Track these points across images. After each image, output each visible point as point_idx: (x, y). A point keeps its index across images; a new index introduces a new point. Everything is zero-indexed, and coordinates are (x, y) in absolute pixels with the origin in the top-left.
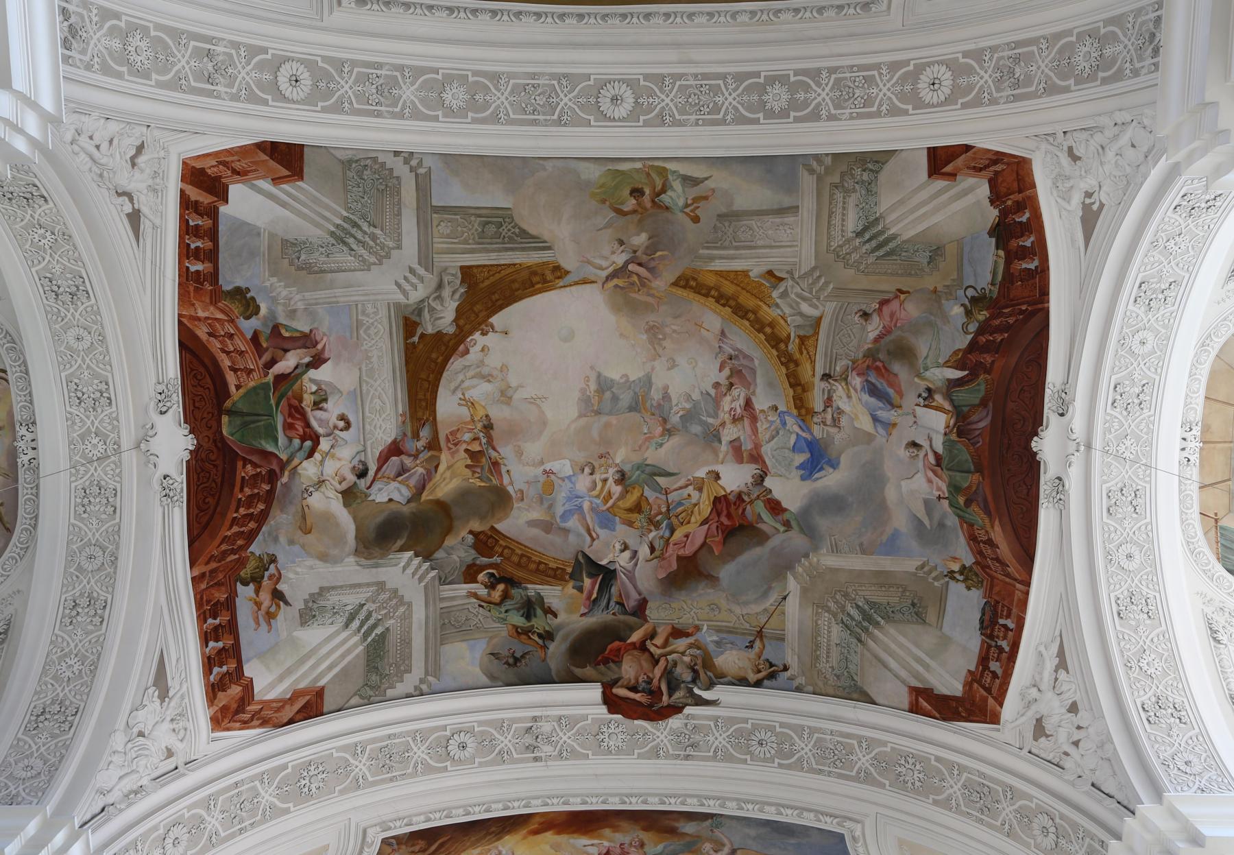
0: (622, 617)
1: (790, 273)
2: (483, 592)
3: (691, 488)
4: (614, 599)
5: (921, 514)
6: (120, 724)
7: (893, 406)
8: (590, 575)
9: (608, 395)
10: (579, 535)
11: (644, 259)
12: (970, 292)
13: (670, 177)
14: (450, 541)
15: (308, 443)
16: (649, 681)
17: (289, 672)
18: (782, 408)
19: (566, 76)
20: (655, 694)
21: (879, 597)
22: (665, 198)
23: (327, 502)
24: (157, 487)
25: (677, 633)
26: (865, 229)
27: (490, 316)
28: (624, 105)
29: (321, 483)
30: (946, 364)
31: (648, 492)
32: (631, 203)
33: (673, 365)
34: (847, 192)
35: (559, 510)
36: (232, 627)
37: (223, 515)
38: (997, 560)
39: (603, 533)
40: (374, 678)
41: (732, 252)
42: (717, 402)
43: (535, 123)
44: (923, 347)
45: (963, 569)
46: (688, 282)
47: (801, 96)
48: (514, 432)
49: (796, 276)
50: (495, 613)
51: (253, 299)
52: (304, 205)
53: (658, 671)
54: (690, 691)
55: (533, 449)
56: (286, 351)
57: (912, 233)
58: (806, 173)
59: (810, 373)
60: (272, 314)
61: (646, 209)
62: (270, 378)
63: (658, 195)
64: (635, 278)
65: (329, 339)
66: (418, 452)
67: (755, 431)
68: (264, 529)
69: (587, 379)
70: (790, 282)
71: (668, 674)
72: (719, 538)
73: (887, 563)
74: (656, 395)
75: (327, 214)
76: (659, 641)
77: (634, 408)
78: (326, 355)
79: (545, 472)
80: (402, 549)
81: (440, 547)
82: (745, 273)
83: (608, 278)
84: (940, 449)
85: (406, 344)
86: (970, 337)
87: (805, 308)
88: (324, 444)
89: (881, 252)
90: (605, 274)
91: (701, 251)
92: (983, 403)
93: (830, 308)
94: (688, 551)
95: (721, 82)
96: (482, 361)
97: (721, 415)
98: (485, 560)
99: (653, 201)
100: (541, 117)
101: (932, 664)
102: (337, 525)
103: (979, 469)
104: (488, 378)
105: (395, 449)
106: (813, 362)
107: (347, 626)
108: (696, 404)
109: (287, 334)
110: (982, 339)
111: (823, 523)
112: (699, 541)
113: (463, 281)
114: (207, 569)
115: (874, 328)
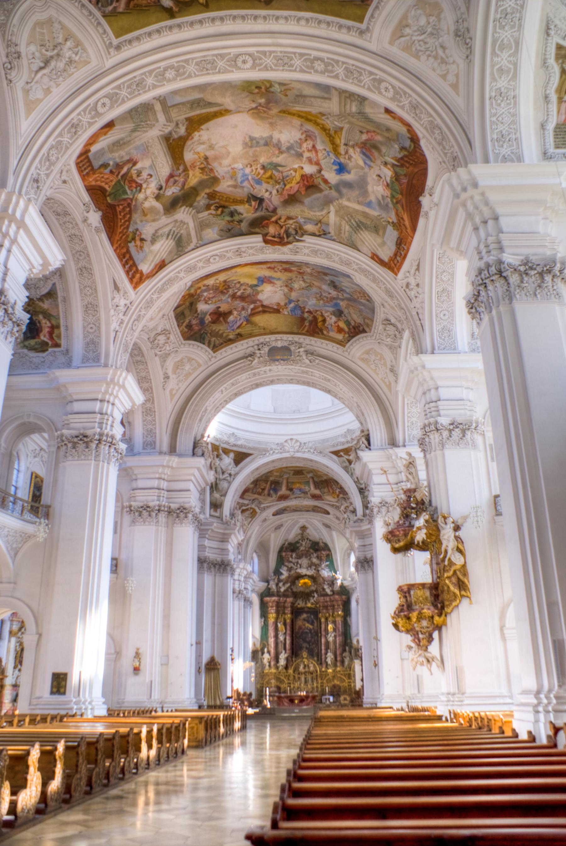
0: (268, 213)
2: (214, 212)
3: (292, 171)
4: (264, 207)
5: (380, 198)
6: (110, 306)
7: (371, 161)
8: (254, 201)
9: (254, 142)
10: (248, 188)
14: (198, 199)
15: (138, 188)
16: (279, 234)
17: (152, 261)
18: (328, 149)
20: (281, 238)
21: (363, 220)
22: (272, 89)
23: (151, 203)
24: (93, 231)
25: (289, 218)
29: (146, 198)
30: (392, 158)
31: (274, 172)
32: (257, 91)
33: (281, 132)
34: (352, 101)
35: (239, 180)
36: (131, 258)
37: (117, 226)
38: (404, 225)
39: (258, 187)
40: (180, 249)
42: (301, 145)
43: (208, 74)
44: (384, 149)
45: (393, 223)
48: (216, 158)
50: (219, 218)
53: (282, 231)
54: (295, 238)
55: (226, 162)
60: (115, 162)
62: (119, 177)
66: (180, 174)
67: (317, 155)
68: (132, 222)
69: (245, 138)
71: (286, 232)
72: (304, 189)
73: (367, 210)
74: (275, 141)
76: (282, 220)
77: (266, 144)
79: (233, 169)
80: (181, 207)
81: (195, 201)
82: (310, 112)
84: (389, 182)
85: (168, 145)
87: (336, 123)
88: (144, 186)
92: (405, 175)
93: (346, 126)
94: (292, 192)
98: (213, 202)
100: (211, 72)
101: (379, 249)
102: (156, 209)
103: (402, 194)
104: (203, 143)
105: (171, 176)
106: (340, 139)
107: (167, 238)
108: (292, 145)
110: (406, 159)
111: (344, 190)
112: (296, 189)
114: (117, 245)
115: (364, 137)
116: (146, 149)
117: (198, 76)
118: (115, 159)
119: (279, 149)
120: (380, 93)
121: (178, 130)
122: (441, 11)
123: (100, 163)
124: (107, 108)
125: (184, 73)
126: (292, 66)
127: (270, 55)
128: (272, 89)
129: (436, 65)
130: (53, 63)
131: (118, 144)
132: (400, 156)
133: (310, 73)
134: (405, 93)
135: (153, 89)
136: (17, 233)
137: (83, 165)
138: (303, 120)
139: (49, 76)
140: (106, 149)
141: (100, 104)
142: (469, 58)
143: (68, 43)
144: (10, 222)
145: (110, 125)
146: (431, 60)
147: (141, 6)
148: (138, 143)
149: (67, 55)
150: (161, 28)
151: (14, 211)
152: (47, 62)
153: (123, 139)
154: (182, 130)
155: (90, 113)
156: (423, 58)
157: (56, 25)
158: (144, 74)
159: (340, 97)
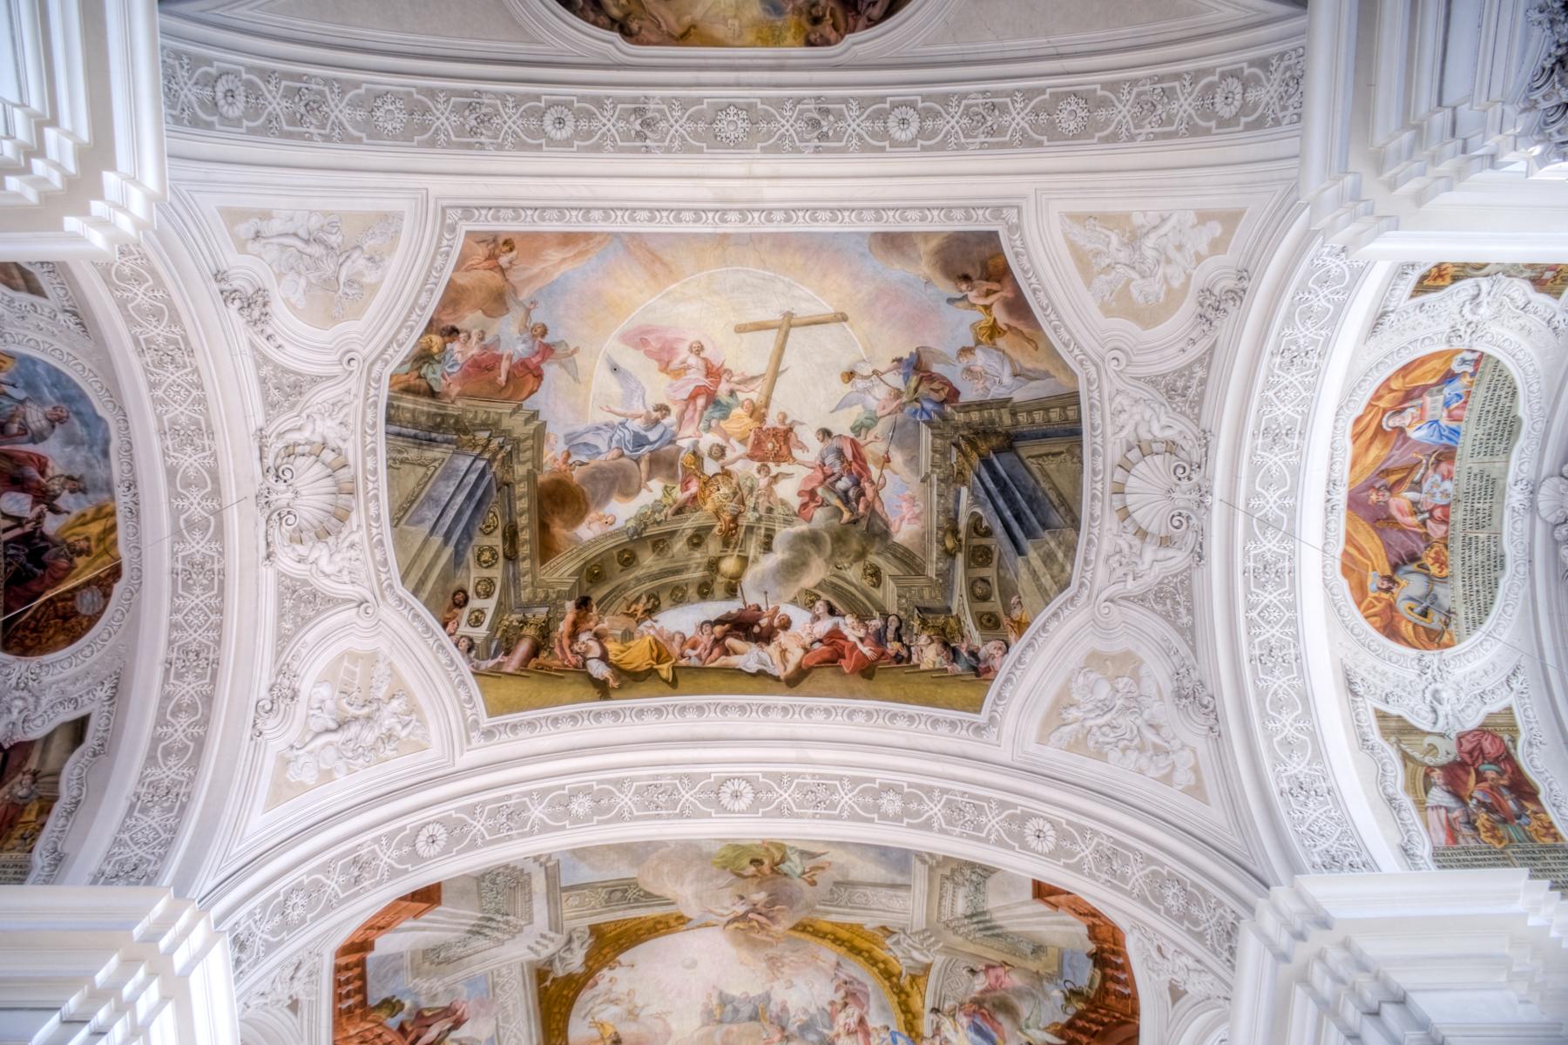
1: (904, 931)
9: (729, 1008)
11: (764, 910)
12: (1069, 985)
13: (788, 852)
18: (892, 1029)
19: (688, 776)
22: (784, 867)
26: (972, 916)
27: (617, 955)
28: (745, 800)
30: (1046, 1029)
32: (752, 870)
33: (790, 985)
41: (847, 910)
42: (832, 1018)
43: (659, 817)
44: (1025, 1009)
46: (802, 927)
47: (914, 806)
49: (908, 932)
51: (398, 1001)
52: (443, 922)
56: (429, 1026)
57: (1016, 929)
58: (918, 863)
59: (920, 1005)
60: (416, 1004)
61: (765, 875)
63: (777, 864)
64: (755, 924)
65: (466, 1001)
69: (710, 995)
70: (902, 936)
74: (774, 1008)
75: (463, 921)
77: (754, 1017)
78: (466, 1017)
82: (860, 926)
83: (728, 923)
86: (1068, 1017)
87: (916, 954)
89: (989, 933)
90: (725, 919)
91: (818, 907)
93: (938, 960)
95: (837, 783)
96: (610, 990)
97: (836, 1028)
99: (772, 869)
100: (663, 812)
104: (615, 1002)
106: (923, 997)
109: (429, 1014)
110: (1080, 1023)
113: (591, 934)
115: (980, 983)
116: (489, 990)
117: (637, 818)
118: (417, 994)
119: (783, 1029)
120: (1025, 846)
121: (567, 955)
122: (1139, 663)
123: (385, 994)
124: (436, 848)
125: (609, 809)
126: (833, 806)
127: (791, 782)
128: (784, 867)
129: (1144, 762)
130: (354, 729)
131: (435, 958)
132: (1064, 1019)
133: (871, 821)
134: (1082, 830)
135: (540, 832)
136: (155, 1011)
137: (348, 981)
138: (843, 950)
139: (338, 749)
140: (407, 962)
141: (423, 837)
142: (1215, 732)
143: (395, 703)
144: (151, 976)
145: (428, 896)
146: (1133, 755)
147: (550, 668)
148: (477, 970)
149: (389, 722)
150: (581, 713)
151: (174, 946)
152: (342, 725)
153: (446, 946)
154: (576, 962)
155: (399, 847)
156: (1114, 755)
157: (381, 666)
158: (529, 794)
159: (931, 880)
